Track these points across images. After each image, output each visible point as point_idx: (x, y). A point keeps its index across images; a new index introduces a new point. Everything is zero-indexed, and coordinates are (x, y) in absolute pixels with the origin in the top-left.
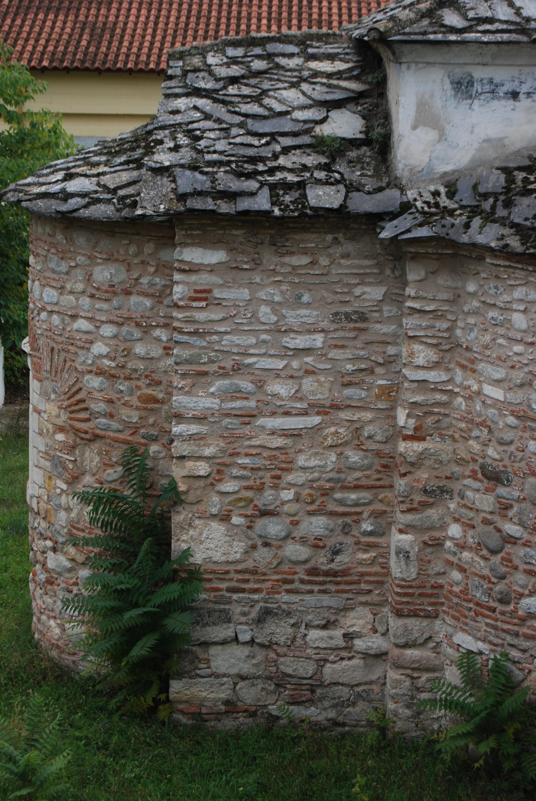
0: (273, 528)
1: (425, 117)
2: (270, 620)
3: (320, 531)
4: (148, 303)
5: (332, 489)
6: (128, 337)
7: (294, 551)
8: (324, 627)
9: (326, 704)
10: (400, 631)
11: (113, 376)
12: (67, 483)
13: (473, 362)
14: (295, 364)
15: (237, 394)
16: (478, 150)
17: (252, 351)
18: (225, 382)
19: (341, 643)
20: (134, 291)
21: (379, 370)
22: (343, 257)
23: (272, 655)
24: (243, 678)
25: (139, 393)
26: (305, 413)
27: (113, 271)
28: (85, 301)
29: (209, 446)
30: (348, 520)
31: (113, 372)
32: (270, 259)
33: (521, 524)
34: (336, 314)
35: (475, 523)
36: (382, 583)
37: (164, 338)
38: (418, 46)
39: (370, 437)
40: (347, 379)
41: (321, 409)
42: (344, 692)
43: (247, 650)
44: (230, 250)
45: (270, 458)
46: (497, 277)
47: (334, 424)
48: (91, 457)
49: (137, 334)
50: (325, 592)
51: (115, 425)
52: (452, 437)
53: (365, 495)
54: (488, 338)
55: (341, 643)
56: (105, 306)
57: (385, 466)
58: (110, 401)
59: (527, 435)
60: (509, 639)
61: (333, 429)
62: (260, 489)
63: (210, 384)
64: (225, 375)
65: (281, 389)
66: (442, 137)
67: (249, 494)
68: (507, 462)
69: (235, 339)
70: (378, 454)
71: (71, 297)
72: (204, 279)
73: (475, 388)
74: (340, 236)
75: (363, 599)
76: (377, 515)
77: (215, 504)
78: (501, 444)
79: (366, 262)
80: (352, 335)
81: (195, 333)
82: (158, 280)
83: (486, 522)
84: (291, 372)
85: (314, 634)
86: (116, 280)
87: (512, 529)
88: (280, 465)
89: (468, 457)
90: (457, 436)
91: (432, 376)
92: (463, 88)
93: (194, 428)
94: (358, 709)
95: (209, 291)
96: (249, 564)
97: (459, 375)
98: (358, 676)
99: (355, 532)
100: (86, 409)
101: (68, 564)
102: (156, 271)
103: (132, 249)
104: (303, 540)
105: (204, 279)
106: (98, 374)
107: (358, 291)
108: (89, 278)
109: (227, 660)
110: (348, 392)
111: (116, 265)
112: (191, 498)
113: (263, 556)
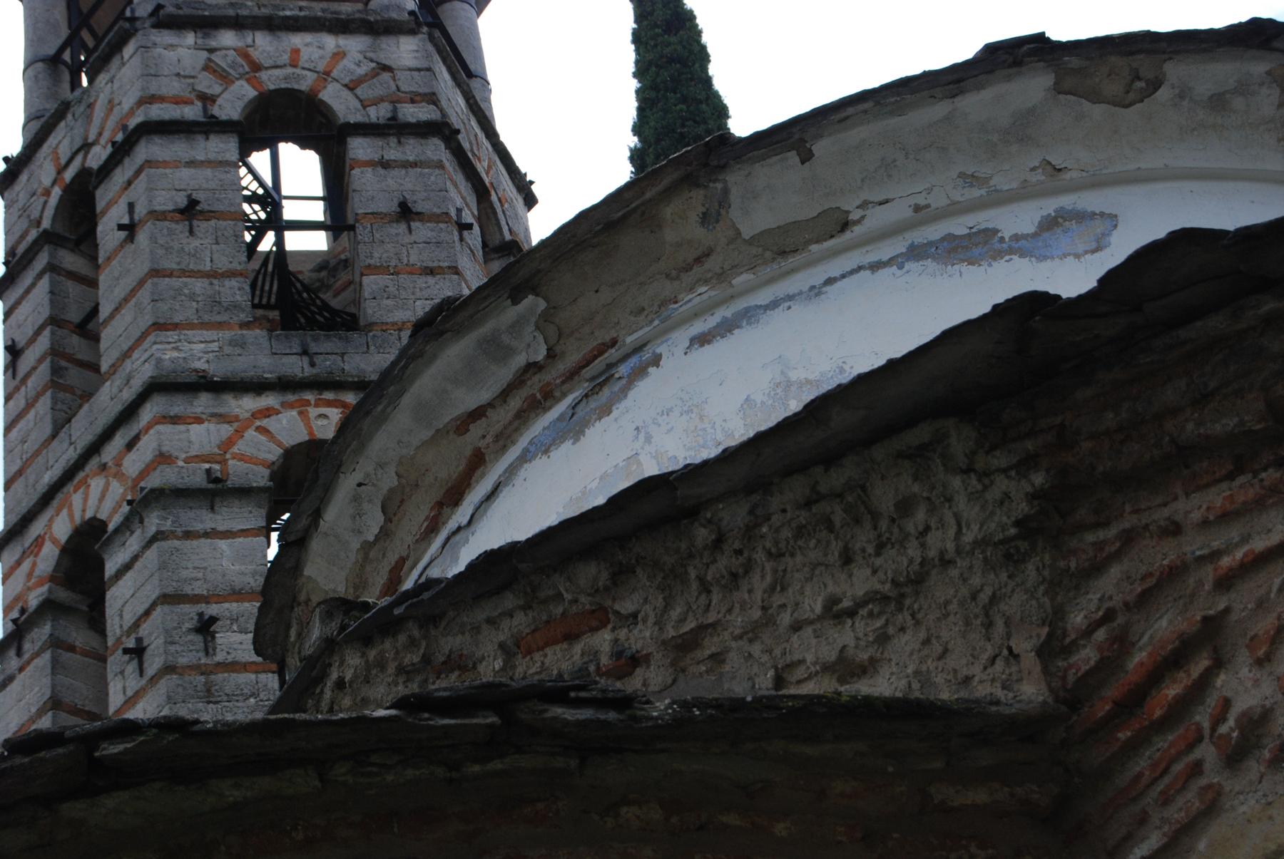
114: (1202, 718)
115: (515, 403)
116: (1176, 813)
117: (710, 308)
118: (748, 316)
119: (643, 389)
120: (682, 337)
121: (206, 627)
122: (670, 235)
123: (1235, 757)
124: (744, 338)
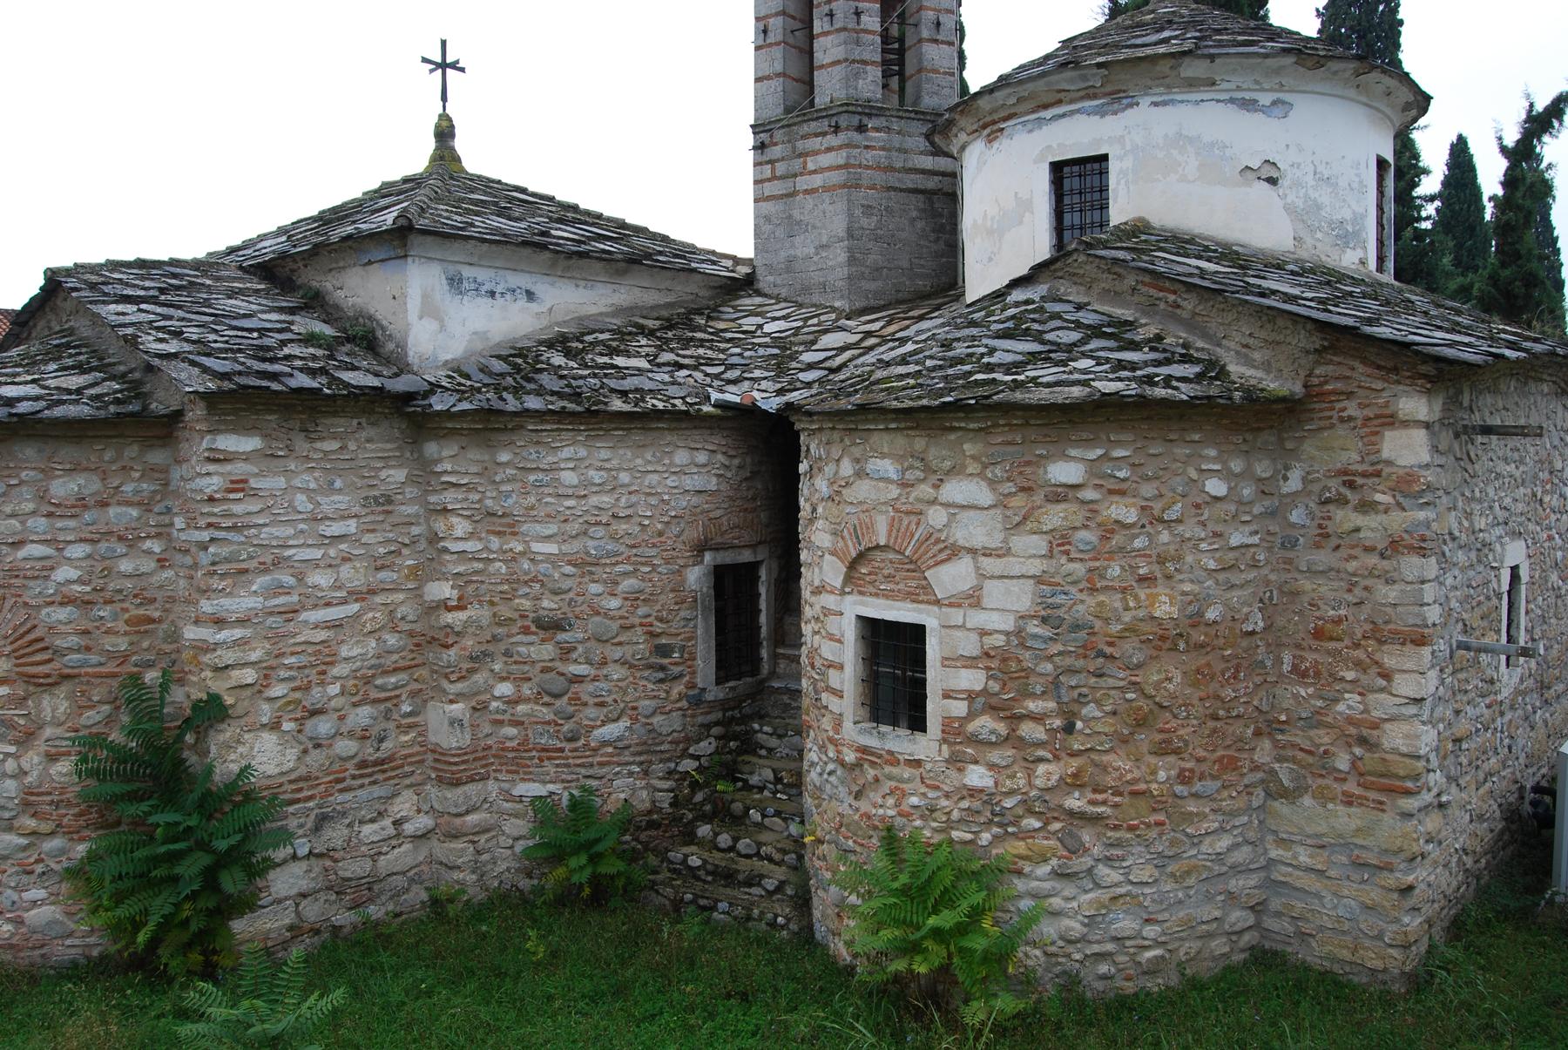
0: (323, 726)
1: (429, 310)
2: (326, 824)
3: (367, 721)
4: (135, 513)
5: (373, 676)
6: (109, 554)
7: (346, 747)
8: (373, 821)
9: (384, 898)
10: (461, 799)
11: (89, 603)
12: (16, 743)
13: (513, 526)
14: (332, 552)
15: (280, 589)
16: (469, 341)
17: (291, 543)
18: (264, 580)
19: (392, 831)
20: (113, 501)
21: (405, 551)
22: (368, 441)
23: (328, 863)
24: (304, 896)
25: (127, 616)
26: (344, 602)
27: (82, 482)
28: (40, 523)
29: (254, 649)
30: (389, 705)
31: (86, 598)
32: (301, 445)
33: (589, 662)
34: (366, 498)
35: (530, 675)
36: (422, 761)
37: (157, 549)
38: (429, 239)
39: (403, 618)
40: (379, 563)
41: (357, 595)
42: (399, 881)
43: (304, 865)
44: (265, 436)
45: (315, 654)
46: (538, 443)
47: (372, 609)
48: (54, 705)
49: (121, 549)
50: (374, 783)
51: (94, 659)
52: (492, 603)
53: (403, 677)
54: (532, 499)
55: (392, 831)
56: (72, 523)
57: (418, 645)
58: (86, 632)
59: (586, 579)
60: (583, 771)
61: (370, 615)
62: (307, 688)
63: (251, 583)
64: (266, 571)
65: (321, 579)
66: (442, 328)
67: (298, 695)
68: (566, 609)
69: (275, 531)
70: (411, 634)
71: (13, 521)
72: (239, 469)
73: (520, 548)
74: (363, 421)
75: (408, 781)
76: (414, 694)
77: (266, 712)
78: (556, 594)
79: (389, 446)
80: (381, 518)
81: (234, 528)
82: (145, 486)
83: (544, 670)
84: (329, 561)
85: (367, 829)
86: (86, 492)
87: (581, 669)
88: (325, 657)
89: (515, 615)
90: (496, 600)
91: (470, 546)
92: (455, 282)
93: (238, 633)
94: (411, 895)
95: (246, 481)
96: (303, 771)
97: (495, 543)
98: (410, 861)
99: (395, 716)
100: (47, 648)
101: (24, 841)
102: (142, 476)
103: (108, 456)
104: (351, 734)
105: (239, 469)
106: (61, 604)
107: (383, 474)
108: (42, 496)
109: (285, 881)
110: (382, 575)
111: (84, 475)
112: (240, 710)
113: (316, 758)
114: (1338, 406)
115: (1082, 93)
116: (1322, 424)
117: (1161, 94)
118: (1172, 102)
119: (1129, 112)
120: (1148, 100)
121: (858, 14)
122: (1158, 68)
123: (1342, 420)
124: (1168, 108)
